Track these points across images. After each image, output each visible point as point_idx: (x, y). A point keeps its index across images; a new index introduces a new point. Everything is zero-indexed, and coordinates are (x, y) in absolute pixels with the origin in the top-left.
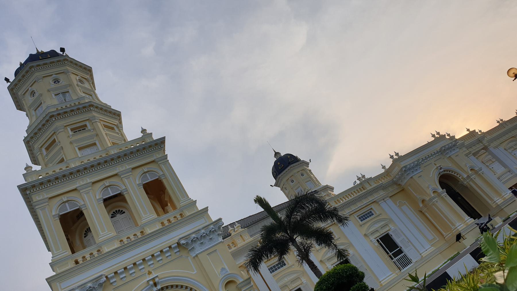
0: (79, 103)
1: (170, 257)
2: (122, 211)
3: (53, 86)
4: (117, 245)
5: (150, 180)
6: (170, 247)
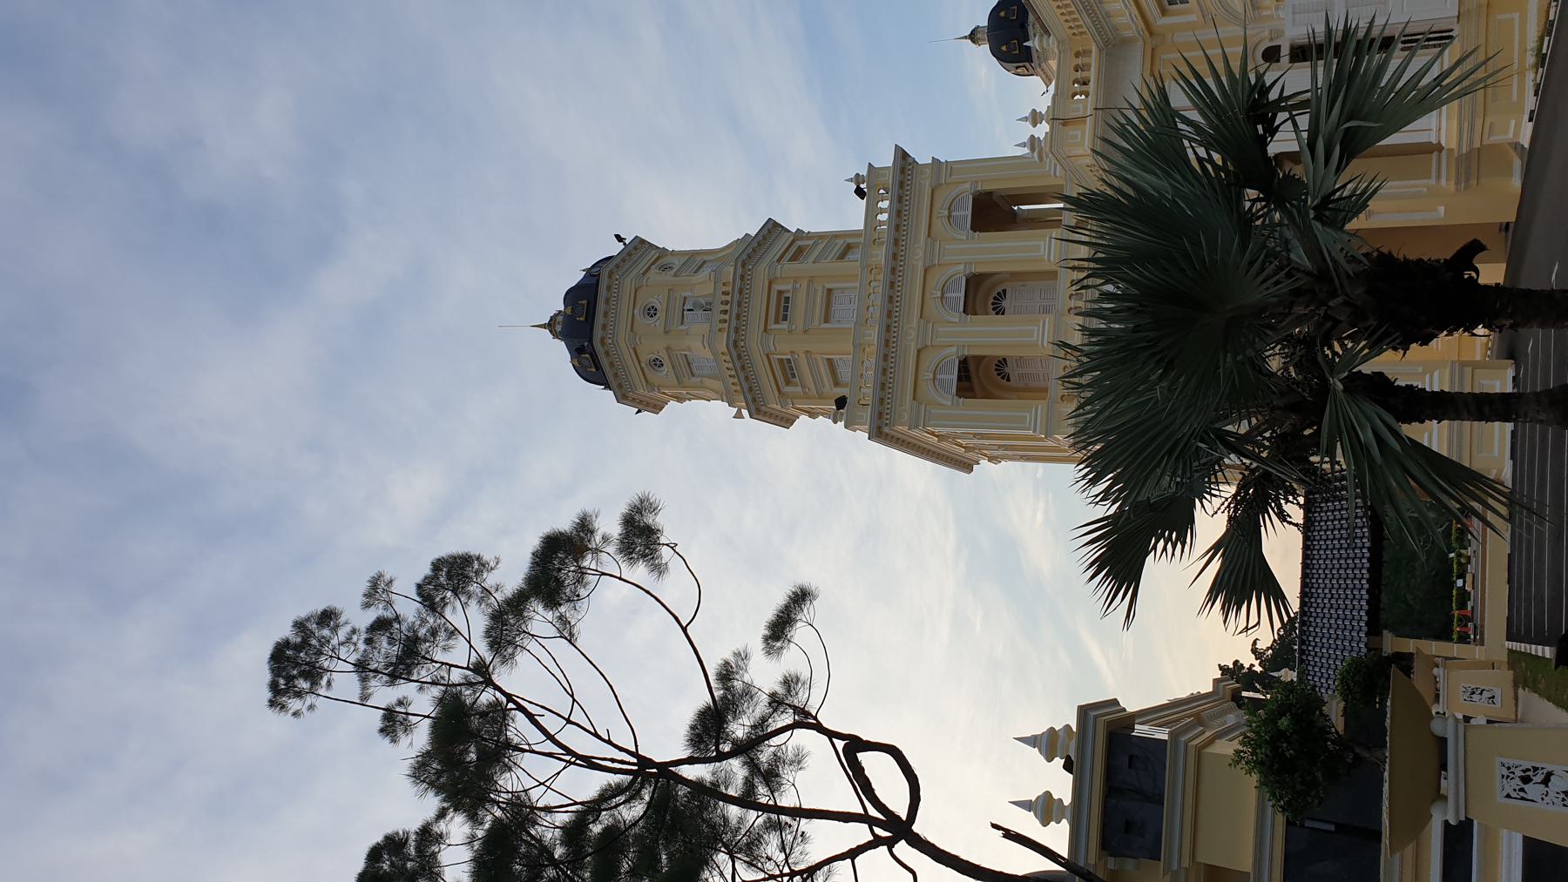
3: (658, 322)
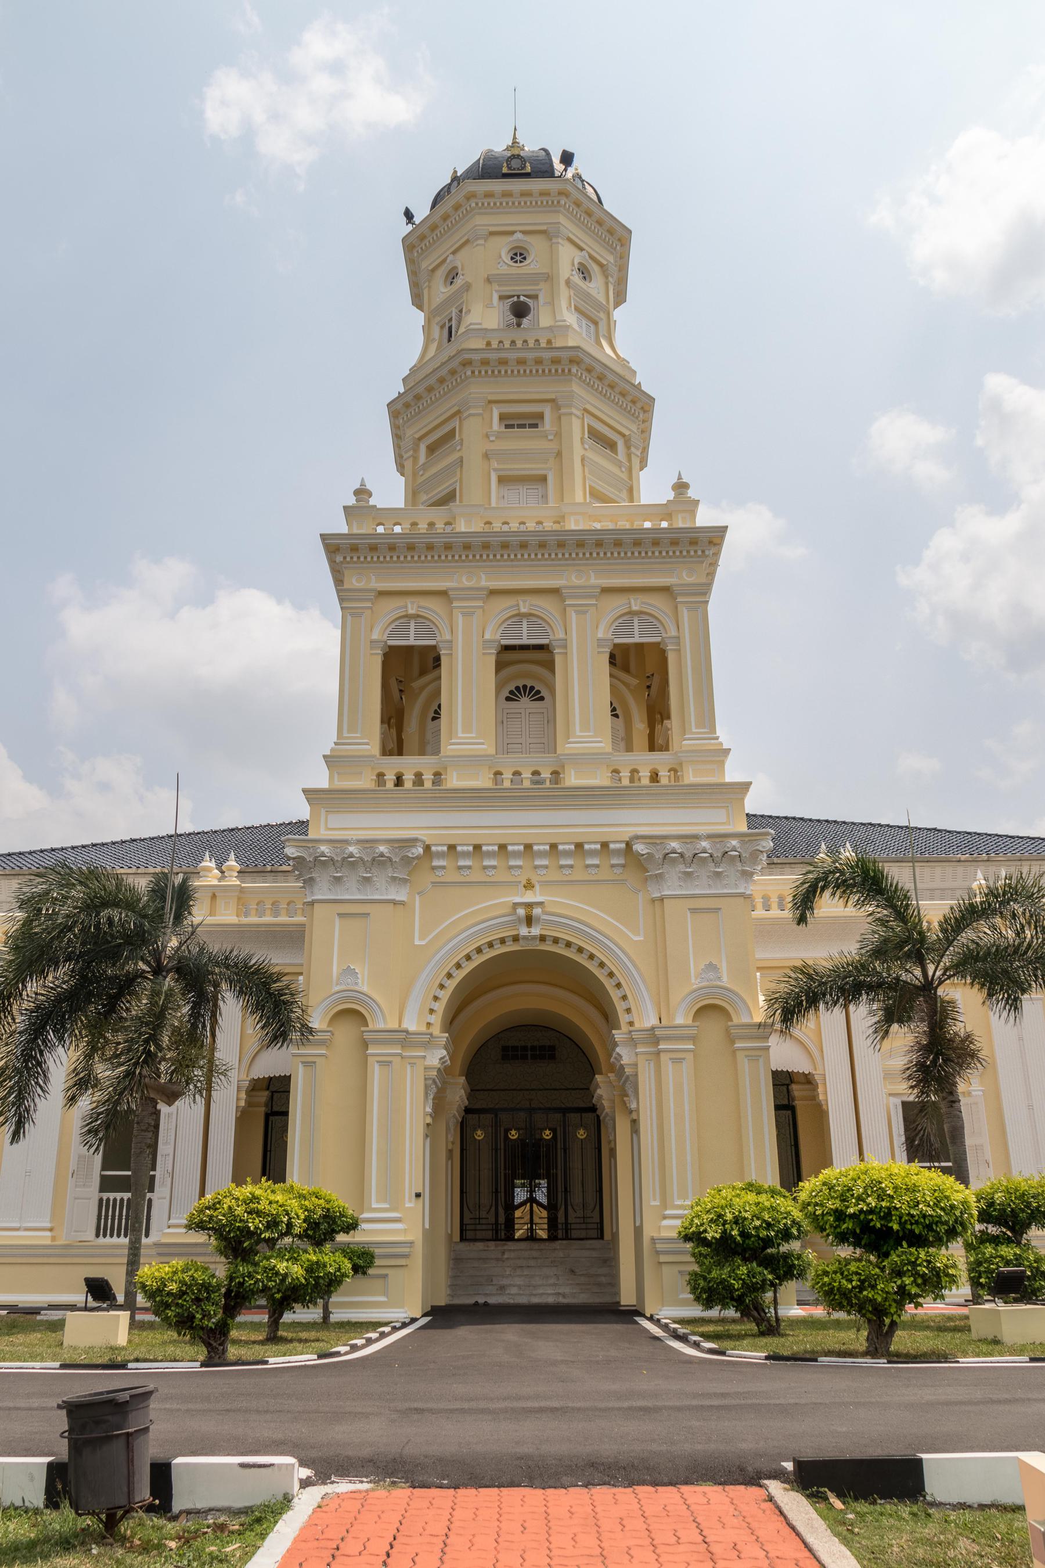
0: (549, 342)
1: (593, 871)
2: (538, 692)
3: (506, 266)
4: (483, 780)
5: (637, 639)
6: (605, 845)
